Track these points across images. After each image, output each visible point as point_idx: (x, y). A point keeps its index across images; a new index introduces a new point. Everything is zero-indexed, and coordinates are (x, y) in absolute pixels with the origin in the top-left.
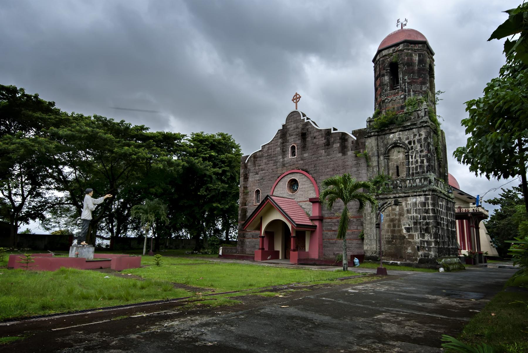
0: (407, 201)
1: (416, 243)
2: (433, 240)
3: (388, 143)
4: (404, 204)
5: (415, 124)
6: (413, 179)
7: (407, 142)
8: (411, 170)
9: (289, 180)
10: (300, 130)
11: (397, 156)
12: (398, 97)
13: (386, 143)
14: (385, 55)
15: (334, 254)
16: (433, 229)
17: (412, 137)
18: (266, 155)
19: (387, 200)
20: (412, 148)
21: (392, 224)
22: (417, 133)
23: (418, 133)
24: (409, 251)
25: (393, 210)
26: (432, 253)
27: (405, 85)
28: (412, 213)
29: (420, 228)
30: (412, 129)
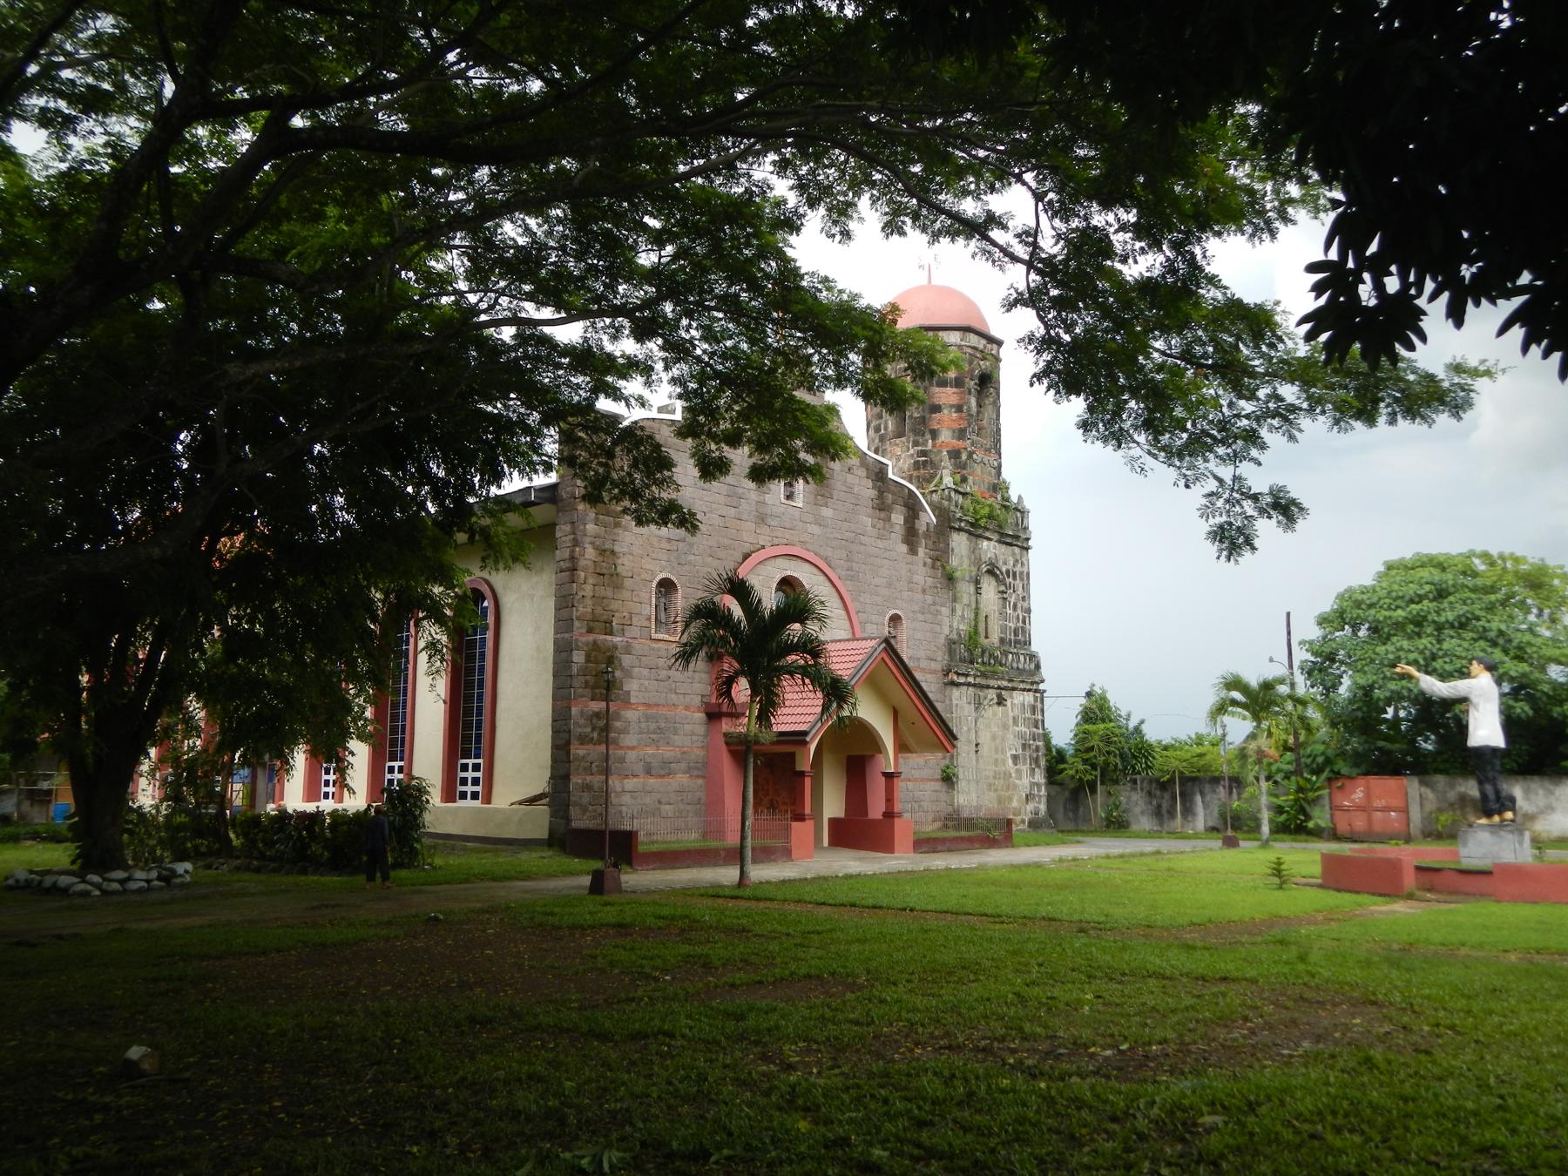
2: (1043, 781)
4: (1009, 703)
5: (1017, 537)
9: (778, 577)
24: (1015, 804)
25: (995, 714)
26: (1043, 807)
30: (1011, 545)
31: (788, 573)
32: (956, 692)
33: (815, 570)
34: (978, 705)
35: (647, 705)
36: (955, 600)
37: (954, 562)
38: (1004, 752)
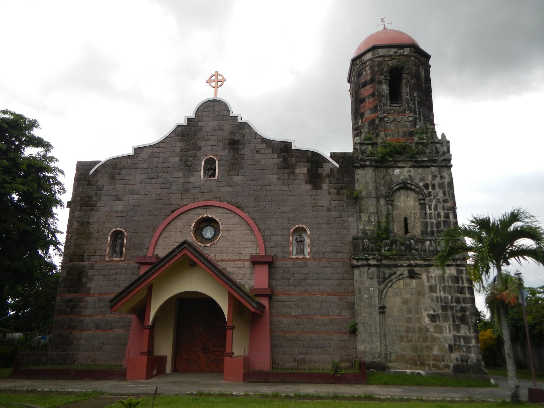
0: (429, 272)
1: (446, 339)
2: (473, 335)
3: (392, 181)
4: (424, 276)
5: (434, 161)
6: (435, 241)
7: (421, 184)
8: (429, 227)
10: (226, 133)
11: (407, 203)
12: (405, 118)
13: (389, 180)
14: (384, 56)
15: (295, 360)
16: (471, 318)
17: (430, 179)
18: (145, 166)
19: (395, 269)
20: (430, 194)
21: (405, 307)
22: (437, 174)
23: (440, 174)
24: (436, 351)
26: (473, 356)
27: (414, 104)
28: (438, 291)
29: (453, 315)
30: (428, 167)
31: (205, 216)
32: (356, 272)
33: (227, 211)
34: (384, 280)
35: (100, 294)
36: (360, 211)
37: (357, 187)
38: (417, 312)
